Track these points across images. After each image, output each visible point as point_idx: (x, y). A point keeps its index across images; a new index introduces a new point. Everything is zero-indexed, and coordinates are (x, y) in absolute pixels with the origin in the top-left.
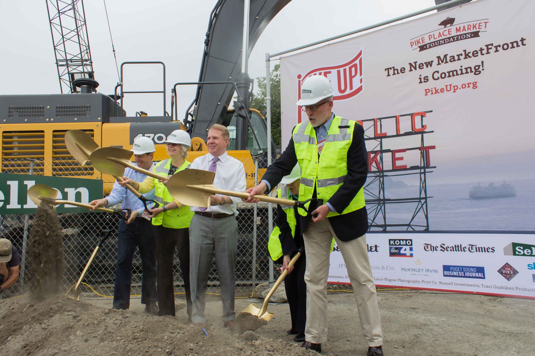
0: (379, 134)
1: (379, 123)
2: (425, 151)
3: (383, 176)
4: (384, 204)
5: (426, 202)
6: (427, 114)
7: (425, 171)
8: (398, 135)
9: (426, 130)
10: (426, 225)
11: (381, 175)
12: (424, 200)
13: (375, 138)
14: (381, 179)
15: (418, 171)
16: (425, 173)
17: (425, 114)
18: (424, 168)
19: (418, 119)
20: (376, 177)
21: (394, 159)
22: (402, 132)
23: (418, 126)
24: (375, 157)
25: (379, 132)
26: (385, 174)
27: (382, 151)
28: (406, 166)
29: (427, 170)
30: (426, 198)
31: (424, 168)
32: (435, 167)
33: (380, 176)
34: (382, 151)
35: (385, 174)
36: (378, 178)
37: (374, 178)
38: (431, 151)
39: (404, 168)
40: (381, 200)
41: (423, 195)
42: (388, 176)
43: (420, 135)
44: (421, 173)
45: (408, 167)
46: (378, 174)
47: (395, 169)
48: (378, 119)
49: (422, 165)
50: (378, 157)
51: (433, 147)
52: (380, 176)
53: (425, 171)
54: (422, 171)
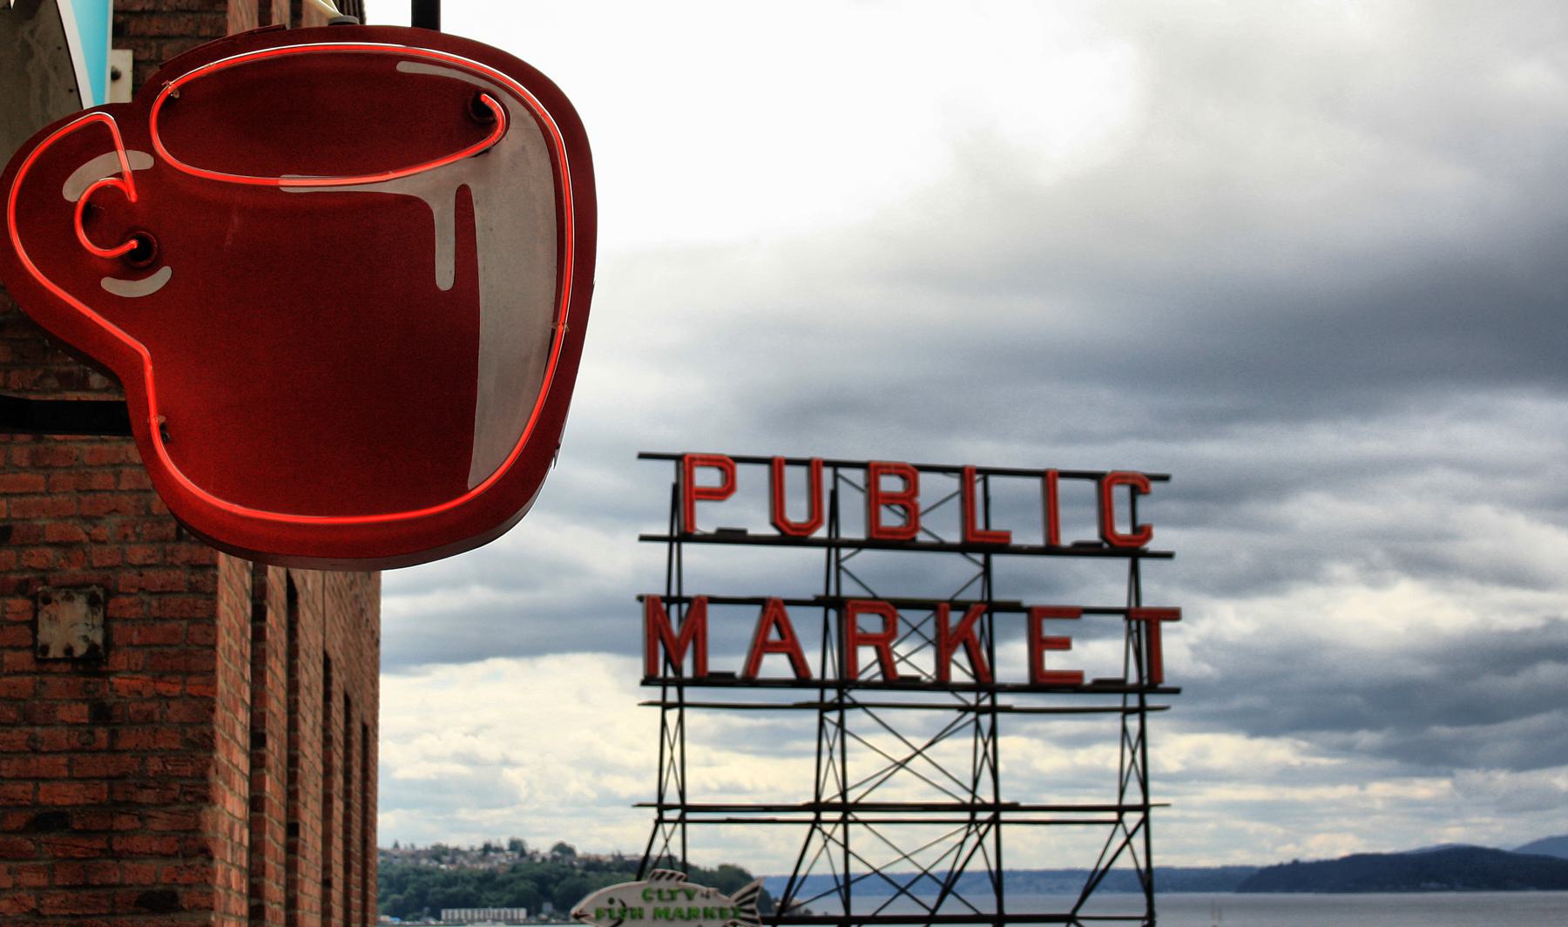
0: (979, 535)
1: (979, 487)
2: (1146, 624)
3: (994, 710)
4: (996, 822)
5: (1145, 821)
6: (1154, 486)
7: (1142, 701)
8: (1052, 549)
9: (1151, 546)
10: (1143, 913)
11: (987, 702)
12: (1138, 816)
13: (963, 548)
14: (985, 720)
15: (1115, 701)
16: (1142, 711)
17: (1147, 487)
18: (1140, 690)
19: (1120, 493)
20: (965, 709)
21: (1038, 646)
22: (1066, 539)
23: (1123, 529)
24: (966, 625)
25: (980, 525)
26: (1003, 700)
27: (992, 607)
28: (1078, 675)
29: (1152, 700)
30: (1145, 808)
31: (1140, 690)
32: (1176, 691)
33: (979, 710)
34: (992, 607)
35: (1003, 700)
36: (971, 715)
37: (955, 714)
38: (1166, 626)
39: (1070, 683)
40: (985, 807)
41: (1133, 797)
42: (1008, 709)
43: (1123, 564)
44: (1126, 711)
45: (1088, 681)
46: (971, 698)
47: (1041, 682)
48: (979, 471)
49: (1133, 678)
50: (976, 627)
51: (1174, 615)
52: (979, 710)
53: (1142, 701)
54: (1133, 701)
